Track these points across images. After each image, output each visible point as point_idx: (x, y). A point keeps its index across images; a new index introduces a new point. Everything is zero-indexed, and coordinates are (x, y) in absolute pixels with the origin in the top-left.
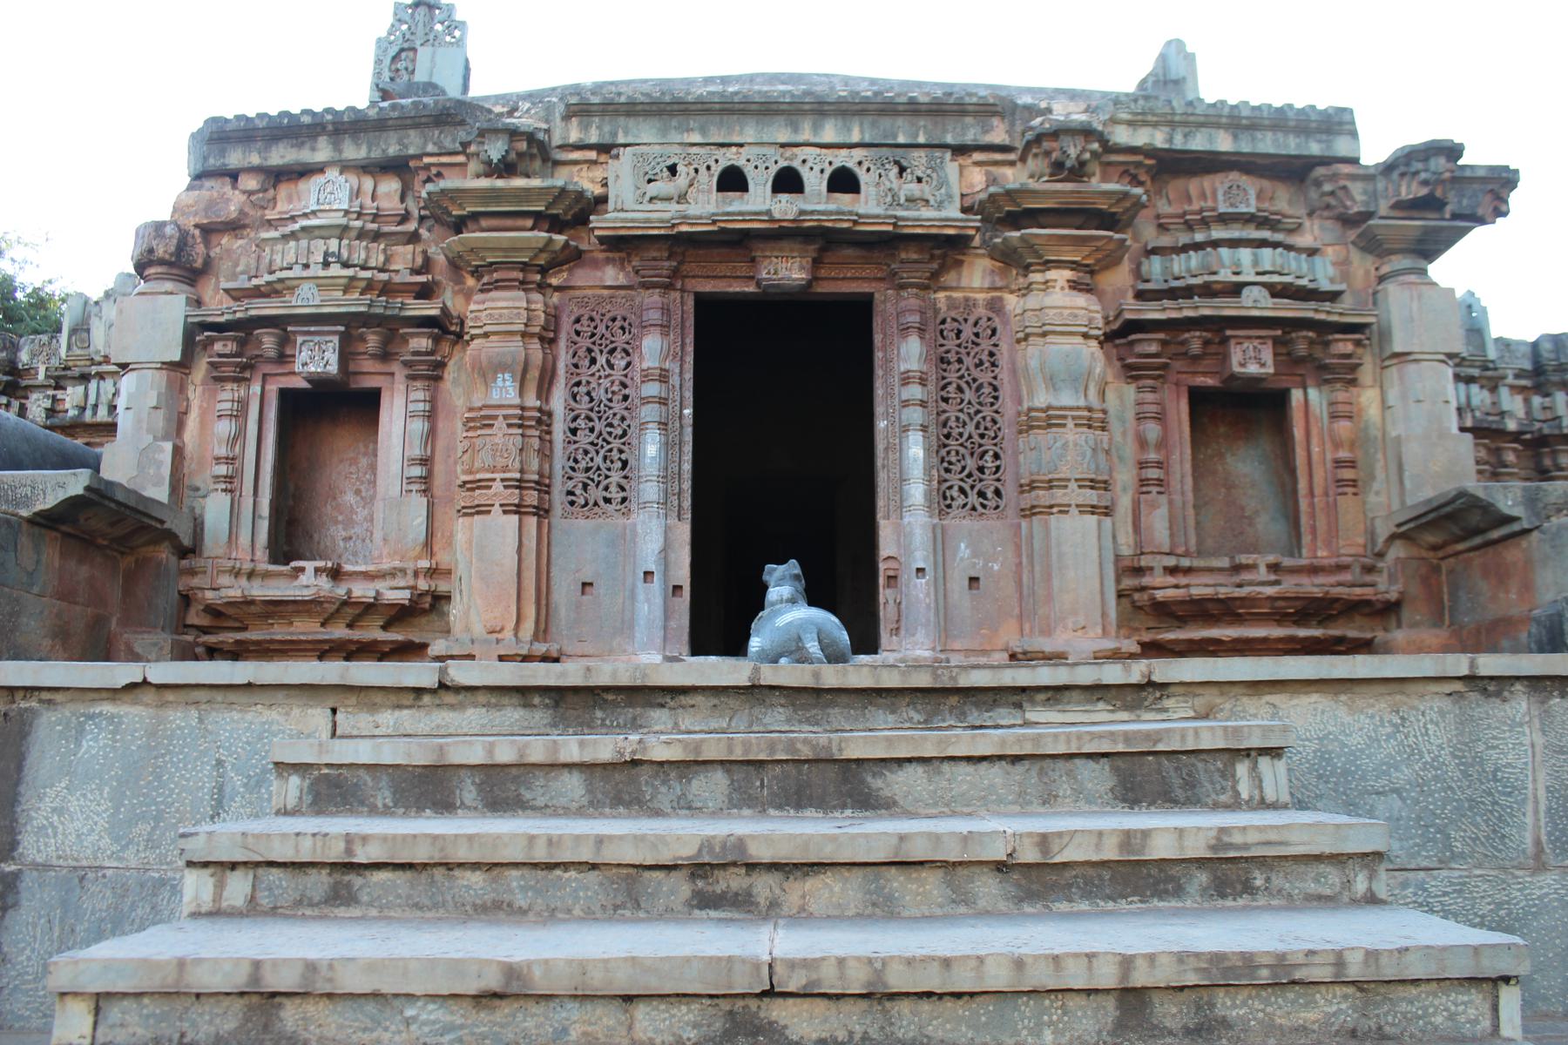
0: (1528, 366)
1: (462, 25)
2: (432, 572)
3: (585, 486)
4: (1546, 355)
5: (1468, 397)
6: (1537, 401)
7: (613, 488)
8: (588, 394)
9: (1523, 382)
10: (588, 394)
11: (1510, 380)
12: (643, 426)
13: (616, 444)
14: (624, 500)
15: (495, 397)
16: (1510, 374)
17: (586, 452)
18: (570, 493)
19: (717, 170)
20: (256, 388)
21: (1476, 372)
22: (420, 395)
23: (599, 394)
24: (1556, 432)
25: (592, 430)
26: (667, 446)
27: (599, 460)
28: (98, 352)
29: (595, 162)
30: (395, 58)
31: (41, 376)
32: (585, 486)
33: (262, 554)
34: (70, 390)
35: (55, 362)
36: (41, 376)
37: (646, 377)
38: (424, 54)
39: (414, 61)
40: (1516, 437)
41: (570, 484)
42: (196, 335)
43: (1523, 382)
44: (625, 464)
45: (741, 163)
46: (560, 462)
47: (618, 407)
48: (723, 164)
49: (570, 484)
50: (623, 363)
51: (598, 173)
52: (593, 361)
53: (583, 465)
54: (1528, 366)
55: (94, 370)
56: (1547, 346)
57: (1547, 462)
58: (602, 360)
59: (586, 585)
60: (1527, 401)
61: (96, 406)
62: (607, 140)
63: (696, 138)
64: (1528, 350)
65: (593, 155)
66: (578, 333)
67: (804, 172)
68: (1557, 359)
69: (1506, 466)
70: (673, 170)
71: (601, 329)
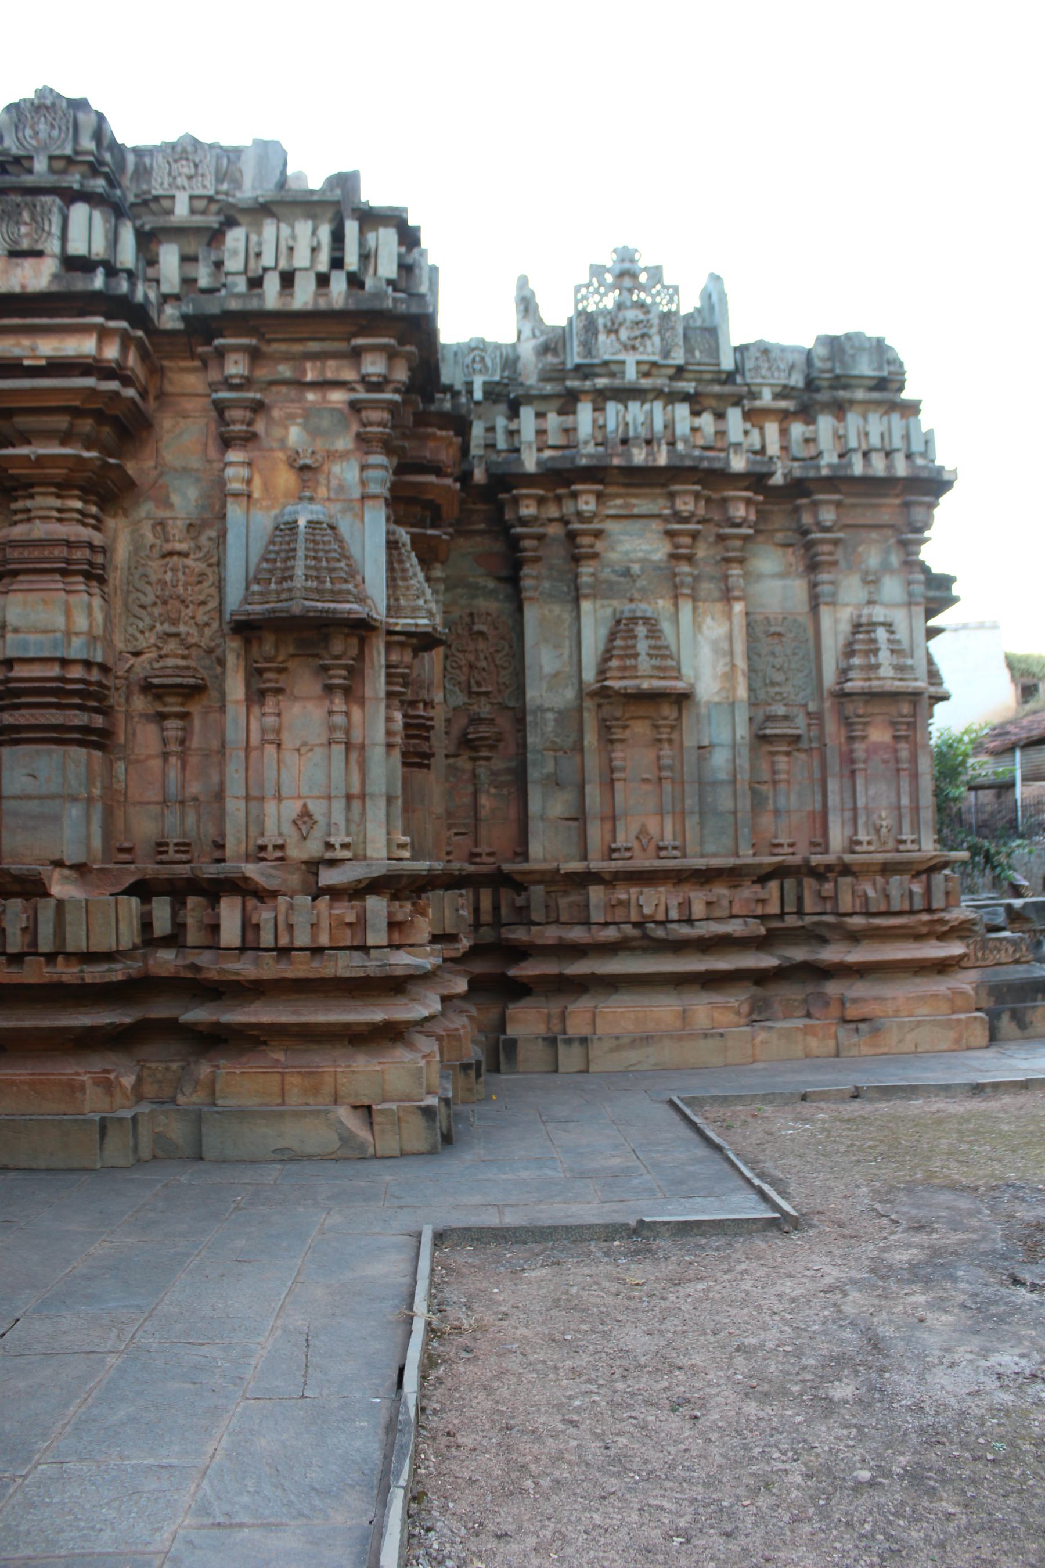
0: (797, 380)
4: (818, 364)
5: (669, 425)
6: (798, 429)
9: (783, 404)
11: (766, 399)
16: (767, 395)
21: (690, 387)
24: (812, 474)
40: (756, 481)
43: (783, 404)
54: (797, 380)
56: (822, 351)
57: (807, 519)
60: (784, 432)
64: (801, 359)
68: (832, 371)
69: (739, 525)
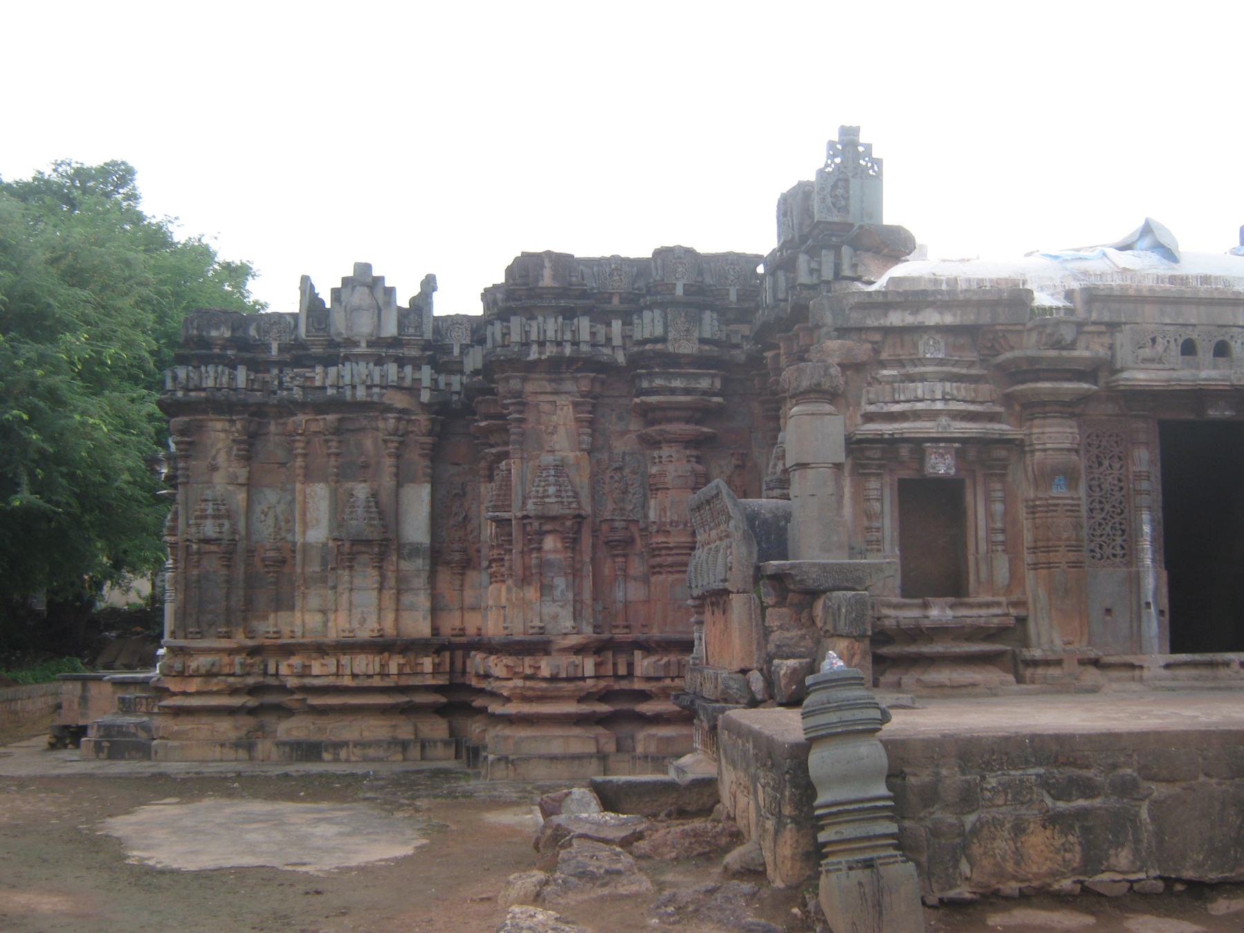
1: (879, 162)
2: (1015, 604)
3: (1101, 547)
7: (1118, 548)
8: (1099, 486)
10: (1099, 486)
12: (1138, 509)
13: (1117, 519)
14: (1124, 555)
15: (1054, 492)
17: (1100, 525)
18: (1092, 551)
19: (1180, 341)
20: (887, 479)
22: (998, 486)
23: (1106, 486)
25: (1102, 509)
26: (1152, 521)
27: (1108, 529)
28: (340, 334)
29: (1100, 333)
30: (835, 187)
31: (274, 351)
32: (1101, 547)
33: (898, 591)
34: (319, 369)
35: (287, 339)
36: (274, 351)
37: (1138, 476)
38: (854, 185)
39: (847, 189)
41: (1092, 545)
42: (855, 445)
44: (1123, 531)
45: (1195, 336)
46: (1085, 533)
47: (1118, 495)
48: (1185, 337)
49: (1092, 545)
50: (1118, 466)
51: (1106, 340)
52: (1100, 464)
53: (1098, 532)
55: (343, 352)
58: (1106, 463)
59: (1108, 611)
61: (354, 387)
62: (1116, 319)
63: (1168, 321)
65: (1103, 328)
66: (1089, 445)
67: (1232, 343)
70: (1154, 340)
71: (1104, 443)
